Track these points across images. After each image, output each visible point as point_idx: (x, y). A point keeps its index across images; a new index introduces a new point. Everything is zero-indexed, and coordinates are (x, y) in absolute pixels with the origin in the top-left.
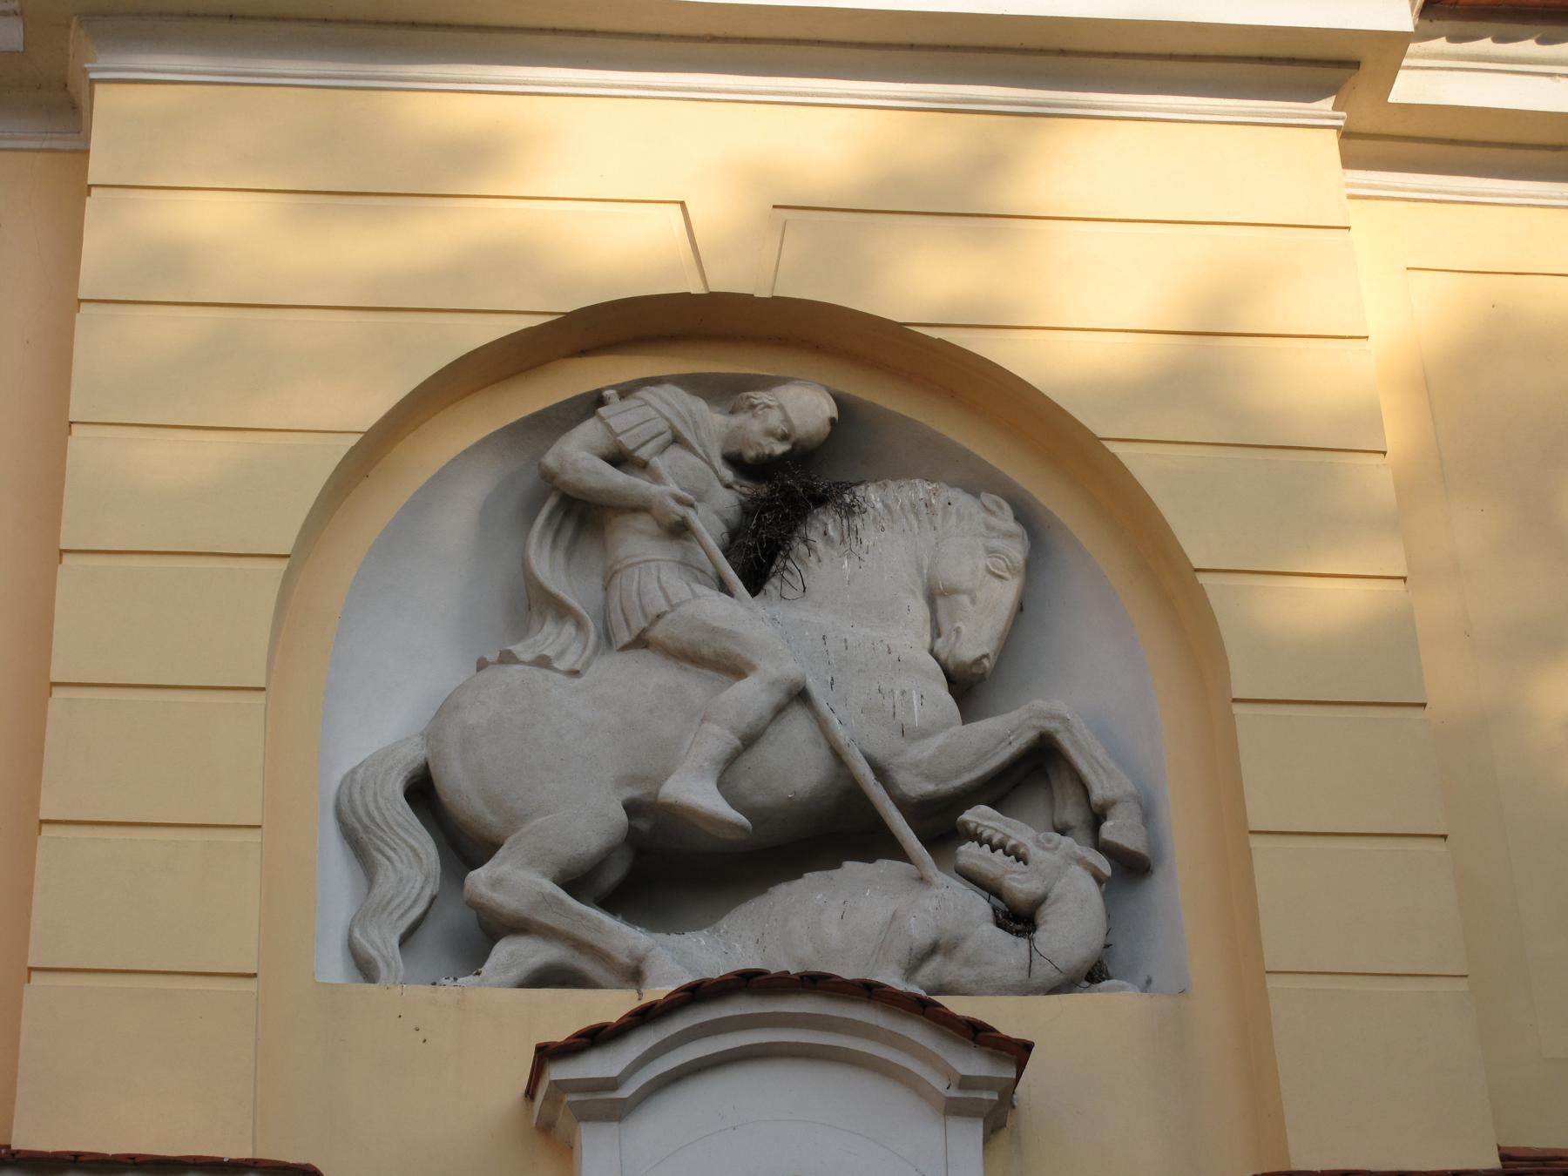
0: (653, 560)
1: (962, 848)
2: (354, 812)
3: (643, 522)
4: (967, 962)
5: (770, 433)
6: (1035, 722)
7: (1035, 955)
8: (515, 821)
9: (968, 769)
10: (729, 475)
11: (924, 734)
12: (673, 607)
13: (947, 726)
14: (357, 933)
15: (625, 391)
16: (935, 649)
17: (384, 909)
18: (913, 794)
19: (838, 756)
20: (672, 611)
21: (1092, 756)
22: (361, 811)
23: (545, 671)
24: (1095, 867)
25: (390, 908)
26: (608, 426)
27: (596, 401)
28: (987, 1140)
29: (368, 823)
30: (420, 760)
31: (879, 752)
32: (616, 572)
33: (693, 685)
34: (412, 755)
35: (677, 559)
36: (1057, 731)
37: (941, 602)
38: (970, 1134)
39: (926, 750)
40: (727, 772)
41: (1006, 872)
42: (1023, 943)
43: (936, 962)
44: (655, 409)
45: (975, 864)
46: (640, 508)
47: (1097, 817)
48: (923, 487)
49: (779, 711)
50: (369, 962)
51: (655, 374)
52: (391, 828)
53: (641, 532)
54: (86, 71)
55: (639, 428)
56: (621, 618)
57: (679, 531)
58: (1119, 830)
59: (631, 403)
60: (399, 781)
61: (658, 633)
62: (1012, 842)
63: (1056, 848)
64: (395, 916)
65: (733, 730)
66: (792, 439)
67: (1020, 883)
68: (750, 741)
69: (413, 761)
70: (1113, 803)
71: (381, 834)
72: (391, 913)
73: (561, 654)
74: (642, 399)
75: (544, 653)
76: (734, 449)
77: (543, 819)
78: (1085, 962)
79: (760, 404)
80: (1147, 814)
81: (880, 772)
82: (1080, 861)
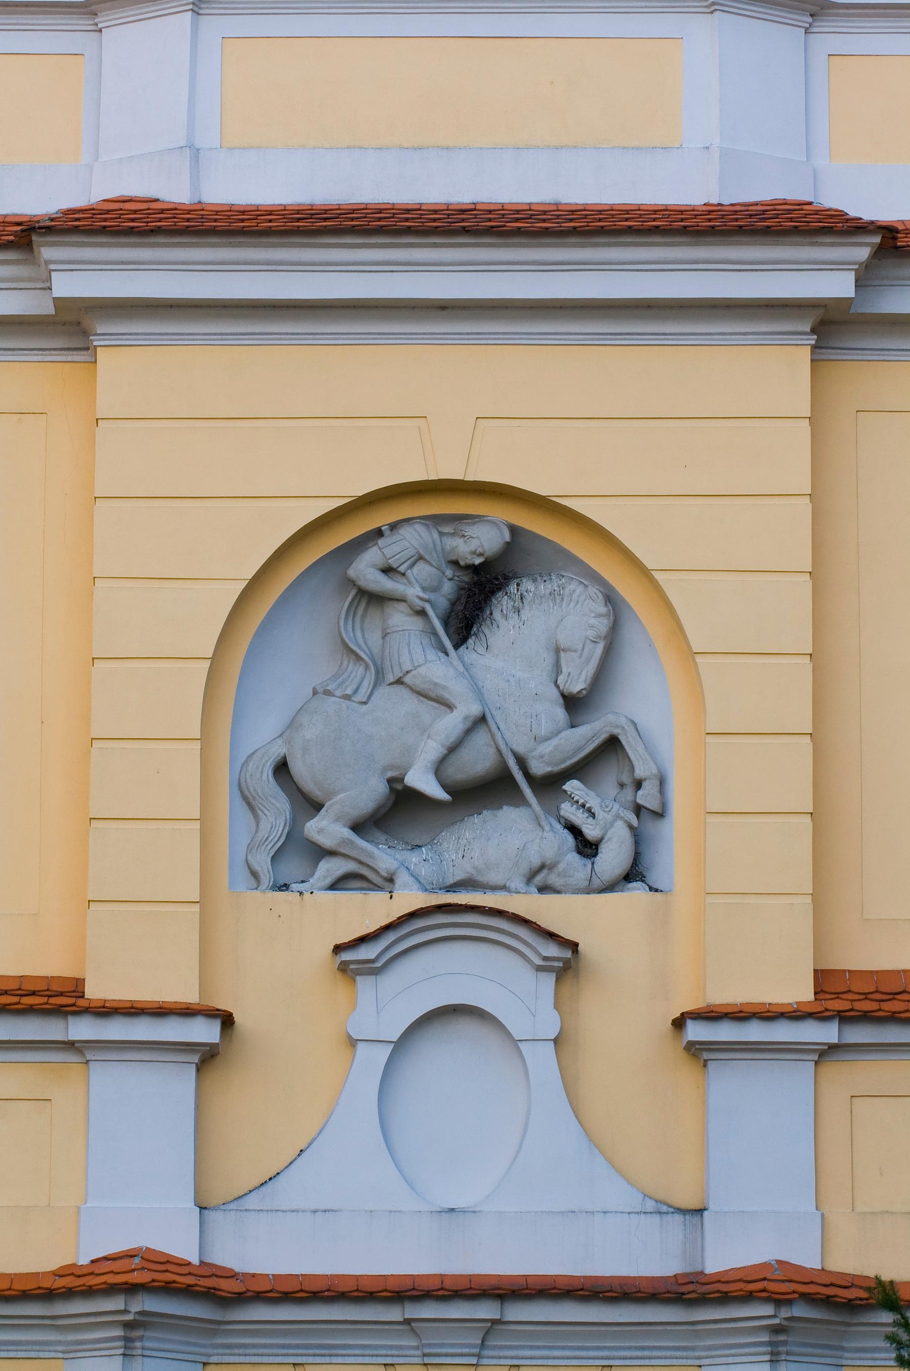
0: (408, 630)
1: (563, 806)
2: (248, 789)
3: (402, 606)
4: (559, 874)
5: (474, 553)
6: (607, 729)
7: (593, 873)
8: (331, 794)
9: (569, 758)
10: (449, 573)
11: (548, 739)
12: (416, 668)
13: (559, 732)
14: (249, 858)
15: (394, 527)
16: (558, 682)
17: (264, 844)
18: (539, 774)
19: (499, 751)
20: (415, 670)
21: (637, 750)
22: (251, 789)
23: (347, 701)
24: (629, 822)
25: (266, 843)
26: (383, 553)
27: (379, 533)
28: (558, 980)
29: (255, 795)
30: (282, 755)
31: (521, 749)
32: (388, 633)
33: (426, 709)
34: (277, 751)
35: (420, 629)
36: (619, 734)
37: (562, 654)
38: (548, 981)
39: (547, 748)
40: (439, 769)
41: (584, 823)
42: (588, 863)
43: (545, 871)
44: (410, 543)
45: (568, 816)
46: (402, 600)
47: (638, 784)
48: (557, 582)
49: (468, 732)
50: (256, 873)
51: (410, 516)
52: (267, 798)
53: (402, 612)
54: (92, 341)
55: (399, 555)
56: (389, 665)
57: (422, 613)
58: (647, 797)
59: (396, 537)
60: (272, 768)
61: (407, 679)
62: (588, 805)
63: (610, 811)
64: (269, 847)
65: (443, 746)
66: (485, 556)
67: (591, 831)
68: (453, 749)
69: (278, 756)
70: (645, 779)
71: (261, 801)
72: (267, 846)
73: (356, 691)
74: (402, 535)
75: (346, 692)
76: (454, 558)
77: (345, 794)
78: (620, 875)
79: (468, 535)
80: (662, 782)
81: (522, 762)
82: (622, 818)
